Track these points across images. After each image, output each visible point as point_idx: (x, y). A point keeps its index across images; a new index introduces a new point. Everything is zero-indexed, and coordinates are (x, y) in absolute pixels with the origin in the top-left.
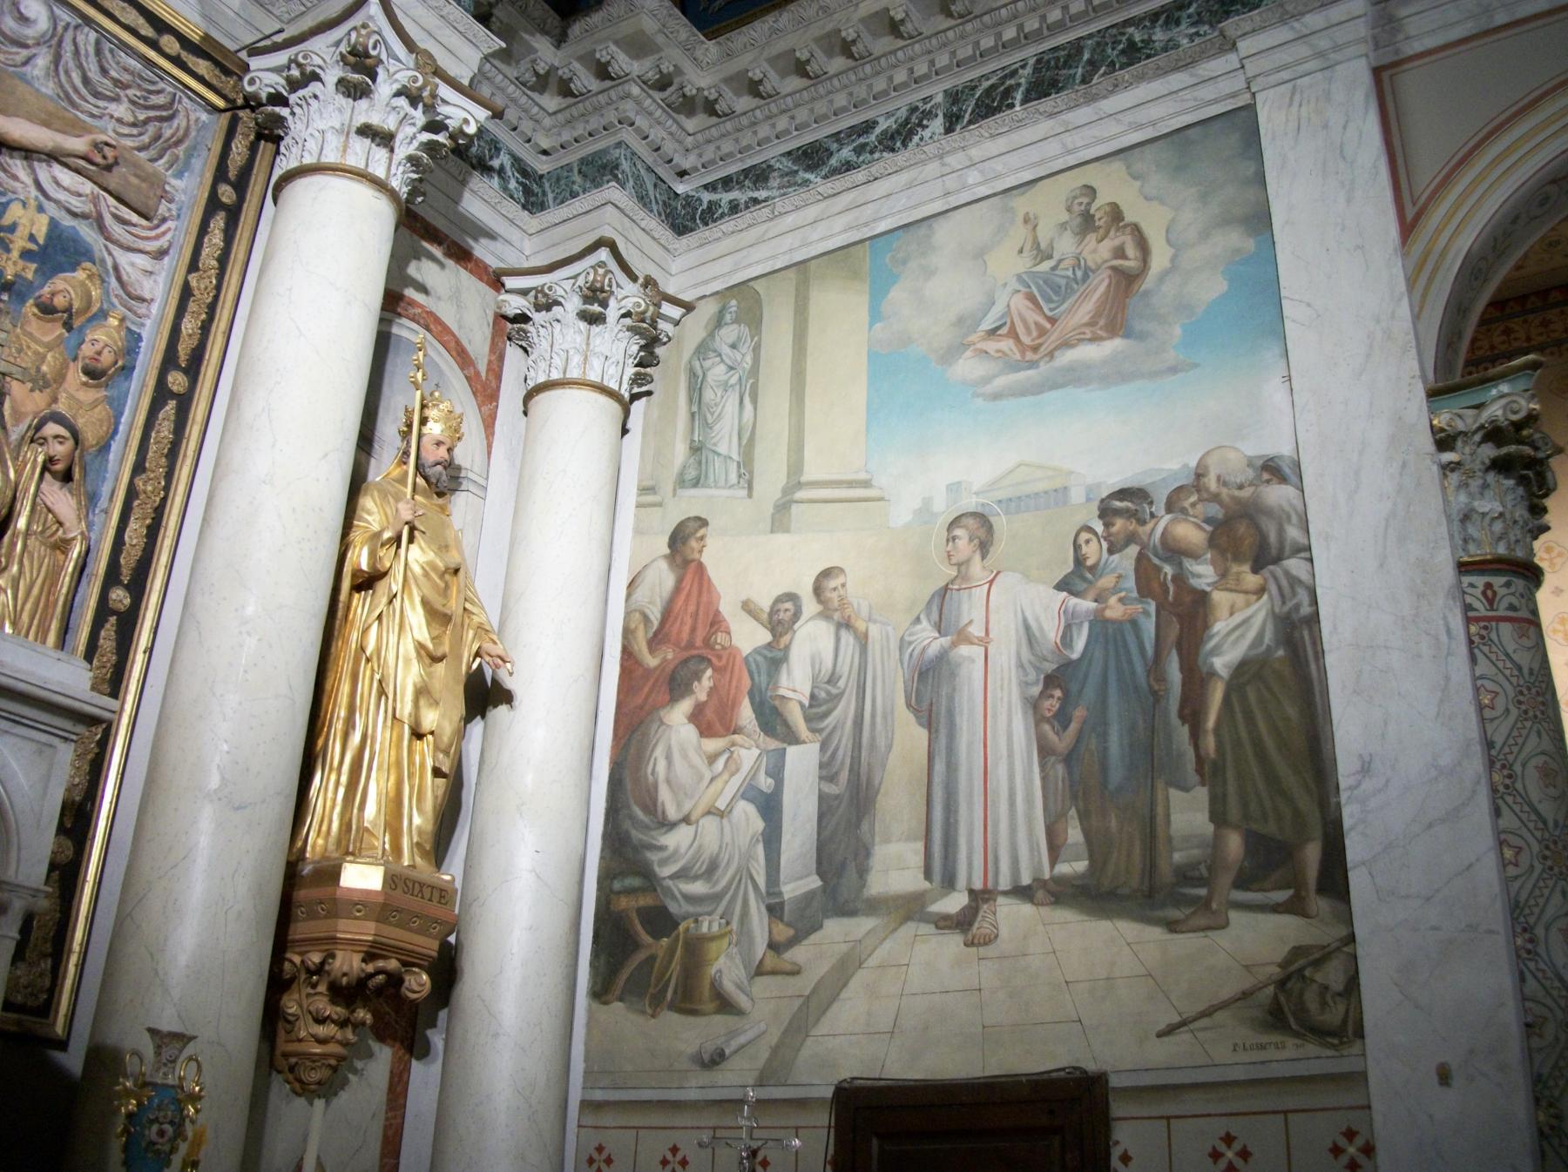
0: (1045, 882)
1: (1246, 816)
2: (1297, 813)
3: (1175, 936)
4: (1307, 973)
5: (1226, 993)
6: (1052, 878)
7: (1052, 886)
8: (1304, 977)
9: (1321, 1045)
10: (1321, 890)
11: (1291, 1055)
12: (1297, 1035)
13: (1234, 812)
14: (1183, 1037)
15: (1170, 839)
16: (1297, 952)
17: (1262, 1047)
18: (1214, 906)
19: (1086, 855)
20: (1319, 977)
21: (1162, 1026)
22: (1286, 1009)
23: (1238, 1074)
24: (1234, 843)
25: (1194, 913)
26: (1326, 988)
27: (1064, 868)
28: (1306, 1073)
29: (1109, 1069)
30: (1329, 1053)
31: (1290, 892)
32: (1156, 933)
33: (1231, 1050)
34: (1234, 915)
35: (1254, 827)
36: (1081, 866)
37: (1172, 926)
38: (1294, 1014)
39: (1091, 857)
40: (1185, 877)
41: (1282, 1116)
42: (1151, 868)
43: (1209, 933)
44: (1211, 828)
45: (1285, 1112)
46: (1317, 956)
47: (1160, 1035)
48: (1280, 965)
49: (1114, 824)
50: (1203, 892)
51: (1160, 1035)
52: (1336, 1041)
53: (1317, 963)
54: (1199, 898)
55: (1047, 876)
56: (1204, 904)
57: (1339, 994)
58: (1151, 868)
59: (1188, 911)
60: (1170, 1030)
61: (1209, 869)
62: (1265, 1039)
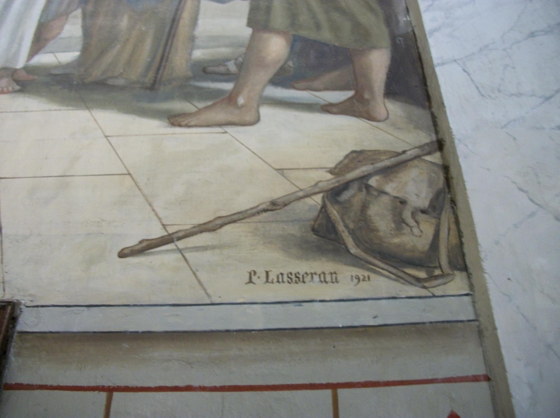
0: (15, 71)
1: (293, 17)
2: (357, 26)
3: (178, 130)
4: (373, 182)
5: (243, 203)
6: (26, 69)
7: (23, 76)
8: (368, 187)
9: (398, 278)
10: (391, 92)
11: (348, 293)
12: (356, 262)
13: (279, 17)
14: (165, 259)
15: (192, 39)
16: (357, 157)
17: (297, 279)
18: (241, 101)
19: (80, 47)
20: (390, 188)
21: (132, 242)
22: (341, 227)
23: (256, 318)
24: (276, 47)
25: (207, 108)
26: (403, 202)
27: (44, 59)
28: (372, 322)
29: (25, 301)
30: (413, 291)
31: (350, 93)
32: (153, 126)
33: (245, 283)
34: (265, 111)
35: (304, 33)
36: (68, 57)
37: (175, 119)
38: (352, 233)
39: (85, 50)
40: (204, 71)
41: (328, 393)
42: (162, 59)
43: (229, 129)
44: (249, 31)
45: (334, 387)
46: (387, 163)
47: (122, 255)
48: (331, 171)
49: (124, 22)
50: (228, 86)
51: (122, 255)
52: (422, 274)
53: (388, 172)
54: (220, 92)
55: (20, 64)
56: (230, 99)
57: (423, 212)
58: (162, 59)
59: (201, 105)
60: (145, 248)
61: (240, 66)
62: (303, 267)
